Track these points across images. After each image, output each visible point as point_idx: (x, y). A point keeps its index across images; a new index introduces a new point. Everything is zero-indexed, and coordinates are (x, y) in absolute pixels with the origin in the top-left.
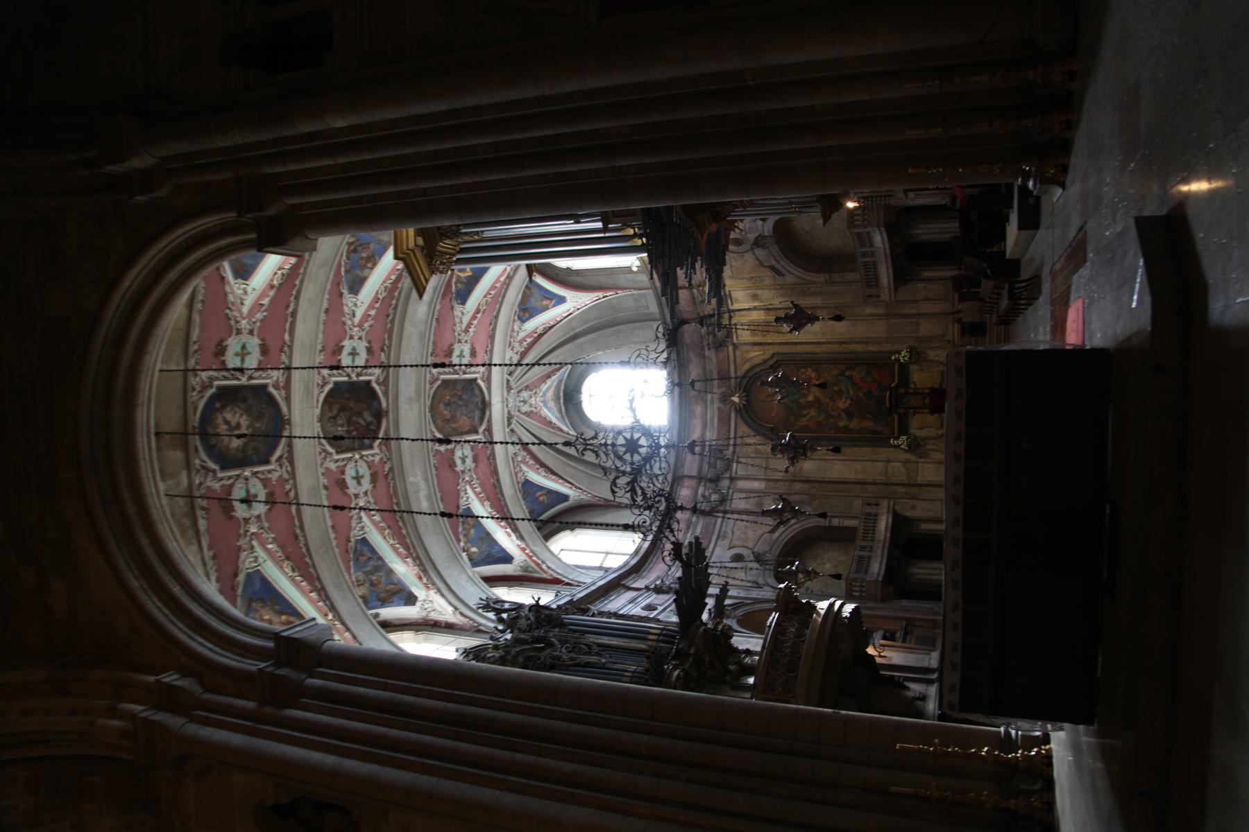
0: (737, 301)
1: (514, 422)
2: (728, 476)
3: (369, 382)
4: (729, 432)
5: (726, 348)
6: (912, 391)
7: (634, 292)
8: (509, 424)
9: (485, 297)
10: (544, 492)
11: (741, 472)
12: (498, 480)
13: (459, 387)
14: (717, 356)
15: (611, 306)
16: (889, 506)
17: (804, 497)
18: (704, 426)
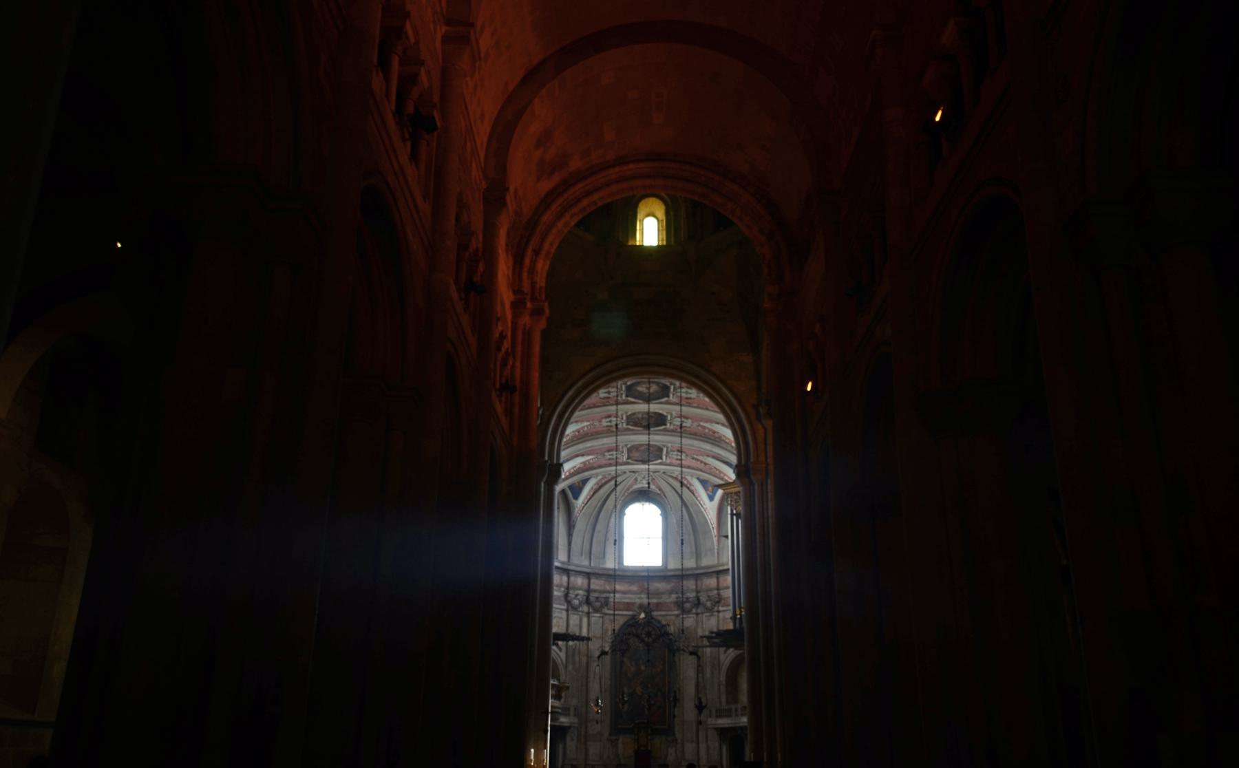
0: (709, 620)
1: (631, 473)
2: (591, 610)
3: (666, 425)
4: (620, 610)
5: (676, 609)
6: (649, 737)
7: (716, 547)
8: (630, 472)
9: (715, 468)
10: (581, 485)
11: (593, 620)
12: (595, 468)
13: (658, 453)
14: (671, 603)
15: (707, 531)
16: (574, 723)
17: (577, 665)
18: (623, 593)
